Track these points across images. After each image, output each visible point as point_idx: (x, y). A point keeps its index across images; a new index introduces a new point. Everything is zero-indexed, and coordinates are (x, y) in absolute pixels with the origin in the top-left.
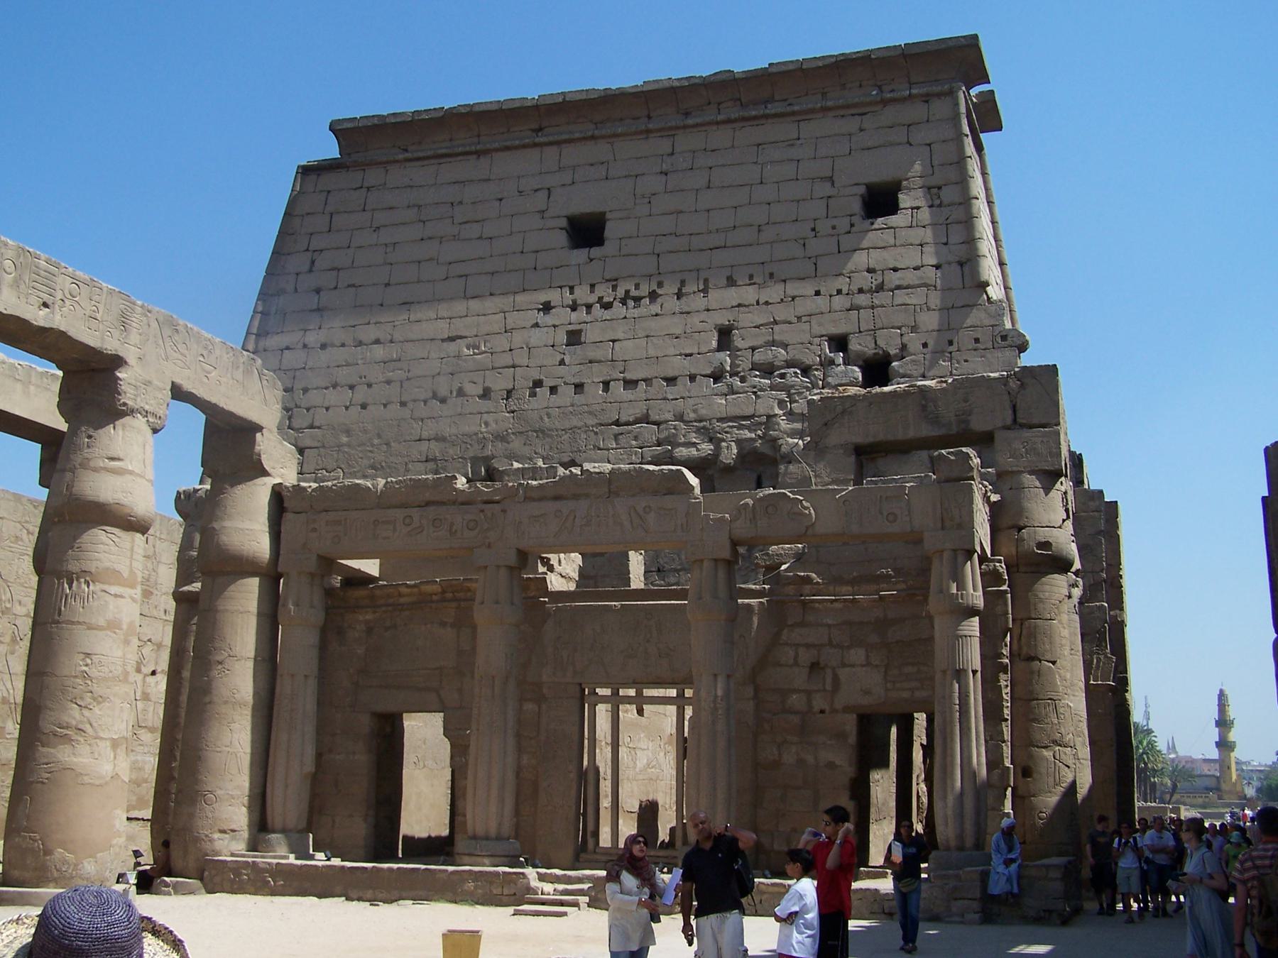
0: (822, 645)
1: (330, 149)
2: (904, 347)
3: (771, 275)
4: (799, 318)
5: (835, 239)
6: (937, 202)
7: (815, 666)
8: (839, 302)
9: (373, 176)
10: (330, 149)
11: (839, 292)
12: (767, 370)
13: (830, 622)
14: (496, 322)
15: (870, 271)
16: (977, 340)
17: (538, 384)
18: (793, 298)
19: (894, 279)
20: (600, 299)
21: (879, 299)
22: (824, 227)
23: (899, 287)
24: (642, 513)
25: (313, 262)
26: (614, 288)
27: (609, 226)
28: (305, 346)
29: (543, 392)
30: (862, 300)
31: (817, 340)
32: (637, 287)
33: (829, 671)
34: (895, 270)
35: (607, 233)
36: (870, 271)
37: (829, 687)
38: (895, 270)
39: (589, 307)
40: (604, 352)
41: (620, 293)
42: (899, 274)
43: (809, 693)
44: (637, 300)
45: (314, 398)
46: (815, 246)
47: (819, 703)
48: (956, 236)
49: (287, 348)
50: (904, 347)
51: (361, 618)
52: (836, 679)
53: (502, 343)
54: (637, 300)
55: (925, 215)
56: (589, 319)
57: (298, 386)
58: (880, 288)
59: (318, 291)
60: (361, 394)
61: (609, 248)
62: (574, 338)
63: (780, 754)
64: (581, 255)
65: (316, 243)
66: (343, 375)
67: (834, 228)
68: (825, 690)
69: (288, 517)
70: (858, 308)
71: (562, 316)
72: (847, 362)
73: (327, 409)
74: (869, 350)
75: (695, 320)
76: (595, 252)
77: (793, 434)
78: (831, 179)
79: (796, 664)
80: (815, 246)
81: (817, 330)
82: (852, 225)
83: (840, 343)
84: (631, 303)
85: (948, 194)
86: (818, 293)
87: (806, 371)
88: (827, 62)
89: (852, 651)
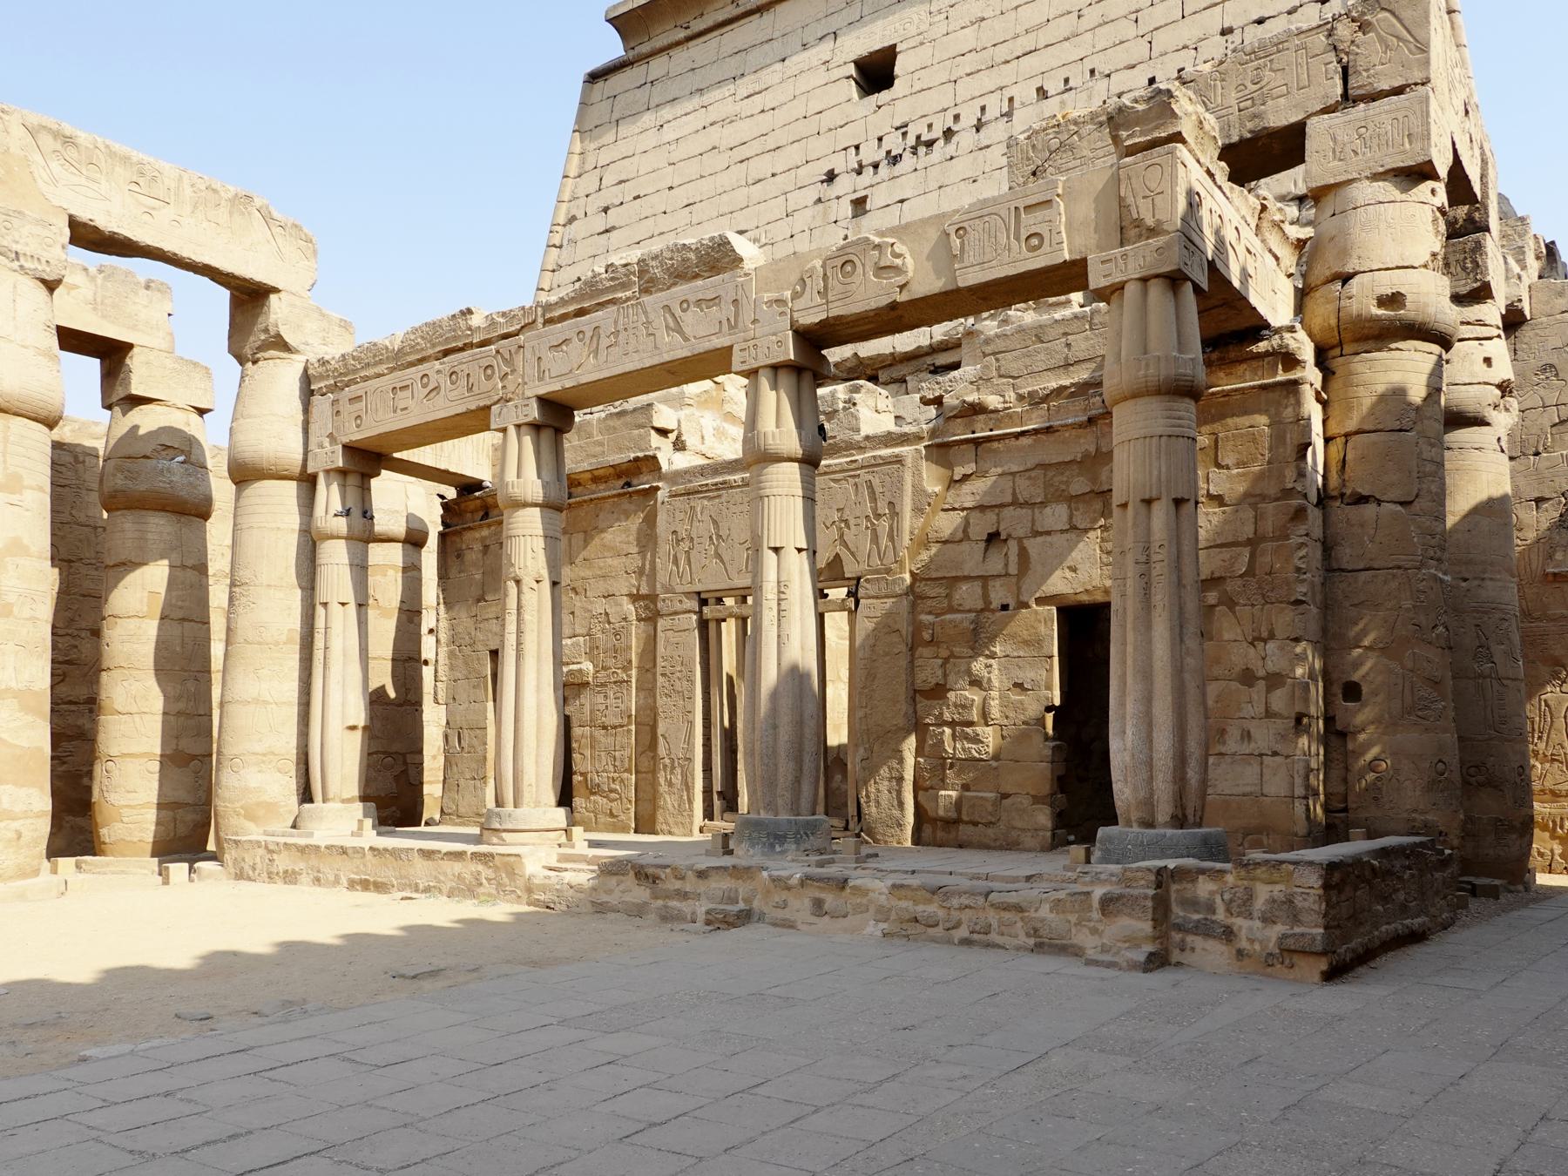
0: (1002, 506)
1: (612, 47)
3: (1092, 72)
7: (993, 538)
9: (657, 66)
10: (612, 47)
13: (1015, 469)
14: (776, 208)
20: (888, 152)
24: (678, 312)
26: (904, 134)
27: (899, 58)
32: (930, 126)
33: (1013, 547)
34: (1260, 22)
35: (897, 70)
37: (1013, 570)
38: (1260, 22)
39: (876, 166)
41: (911, 140)
43: (985, 579)
44: (930, 144)
47: (999, 594)
51: (477, 535)
52: (1023, 554)
54: (930, 144)
56: (878, 179)
62: (859, 205)
63: (945, 675)
68: (1007, 575)
69: (316, 399)
76: (884, 96)
79: (966, 536)
84: (922, 150)
89: (1048, 510)
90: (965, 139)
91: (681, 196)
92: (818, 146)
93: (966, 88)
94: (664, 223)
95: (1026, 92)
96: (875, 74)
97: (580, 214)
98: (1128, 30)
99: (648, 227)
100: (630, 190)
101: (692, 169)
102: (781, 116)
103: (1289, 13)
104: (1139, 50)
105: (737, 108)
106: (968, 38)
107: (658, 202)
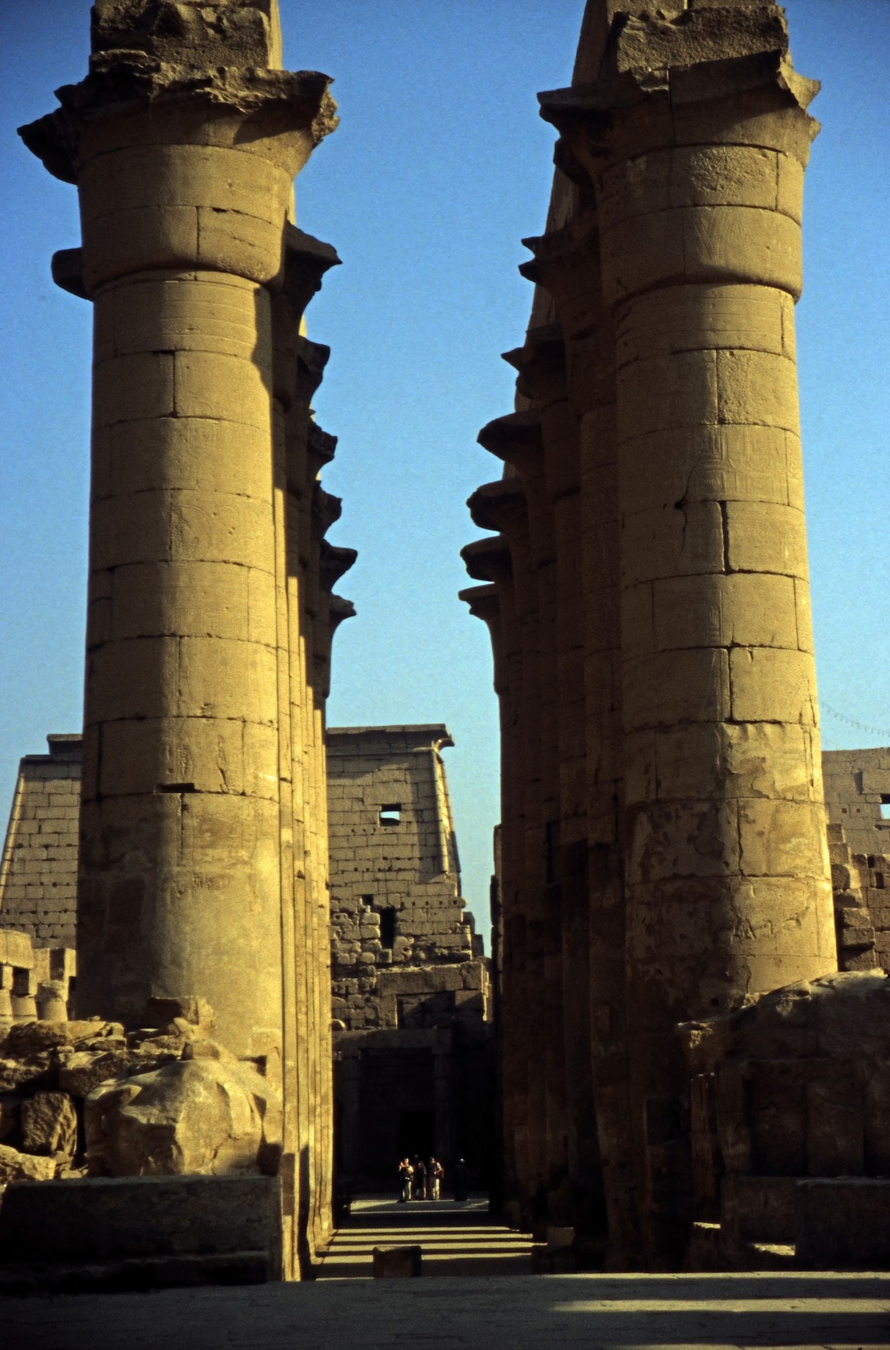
1: (45, 750)
2: (402, 904)
4: (346, 884)
5: (365, 838)
6: (421, 820)
8: (368, 876)
10: (45, 750)
11: (368, 870)
15: (385, 858)
16: (441, 903)
18: (343, 872)
19: (397, 865)
21: (389, 876)
22: (359, 830)
23: (400, 870)
25: (40, 827)
28: (42, 884)
30: (380, 876)
31: (356, 898)
34: (398, 859)
36: (385, 858)
38: (398, 859)
42: (399, 861)
45: (51, 918)
48: (431, 840)
49: (29, 884)
50: (402, 904)
55: (414, 828)
57: (41, 910)
58: (390, 869)
59: (46, 847)
65: (41, 814)
67: (364, 830)
70: (378, 880)
72: (373, 910)
73: (62, 926)
74: (384, 905)
77: (344, 951)
78: (362, 800)
81: (356, 892)
82: (375, 830)
83: (368, 899)
85: (427, 815)
86: (356, 870)
87: (351, 914)
88: (362, 731)
97: (26, 844)
98: (345, 845)
103: (410, 859)
104: (350, 855)
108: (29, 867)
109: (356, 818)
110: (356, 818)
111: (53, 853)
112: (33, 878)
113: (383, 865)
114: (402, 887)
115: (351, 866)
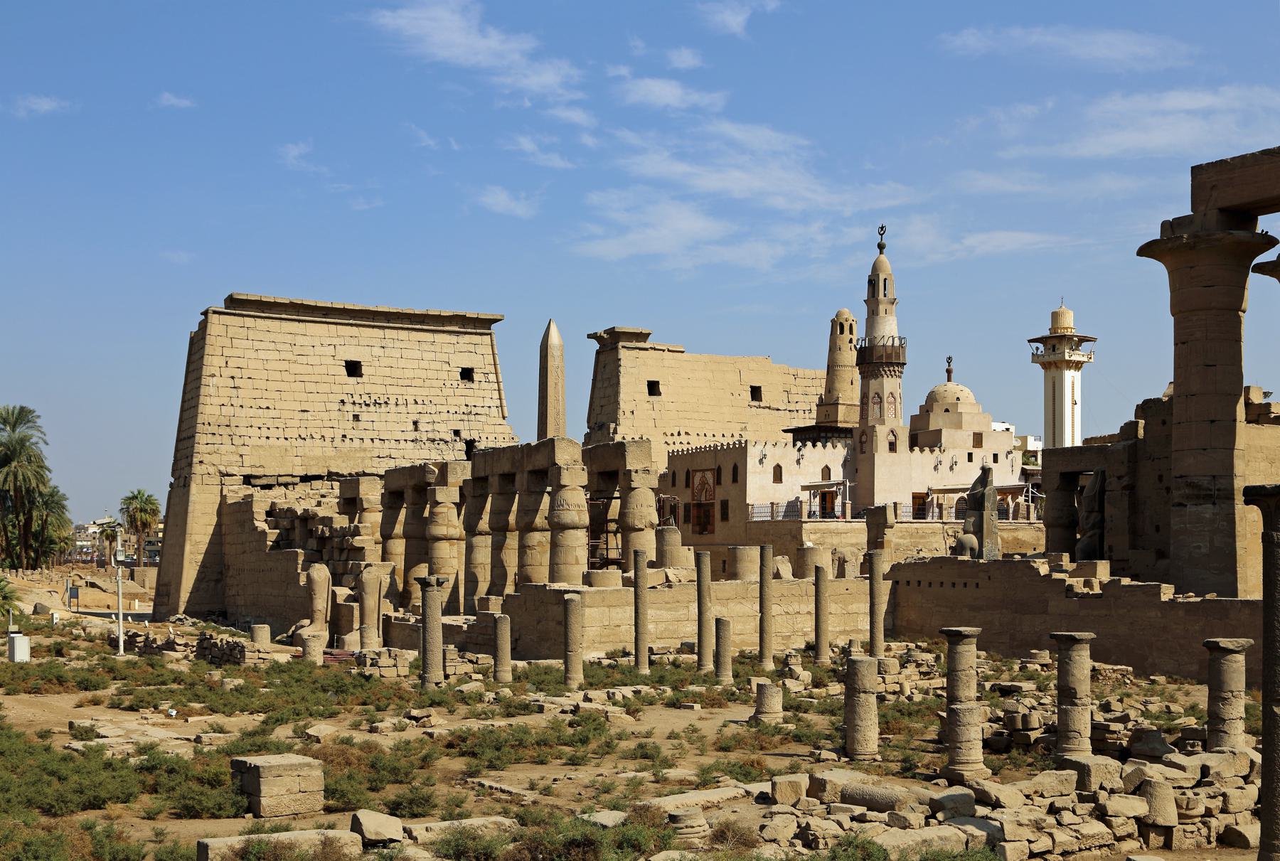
12: (433, 441)
17: (344, 436)
19: (474, 410)
21: (472, 417)
29: (347, 440)
30: (465, 417)
40: (369, 426)
45: (242, 431)
46: (447, 391)
53: (325, 416)
60: (265, 432)
61: (365, 379)
62: (356, 418)
64: (353, 380)
66: (256, 423)
71: (349, 407)
75: (403, 416)
80: (447, 391)
83: (457, 433)
90: (392, 407)
91: (271, 385)
92: (336, 388)
93: (391, 390)
94: (266, 395)
95: (411, 401)
96: (353, 369)
99: (257, 394)
100: (246, 374)
101: (277, 376)
102: (317, 370)
105: (294, 358)
106: (387, 371)
107: (263, 385)
108: (223, 392)
109: (444, 375)
110: (444, 375)
111: (238, 382)
112: (225, 401)
113: (464, 409)
114: (479, 426)
115: (444, 409)
